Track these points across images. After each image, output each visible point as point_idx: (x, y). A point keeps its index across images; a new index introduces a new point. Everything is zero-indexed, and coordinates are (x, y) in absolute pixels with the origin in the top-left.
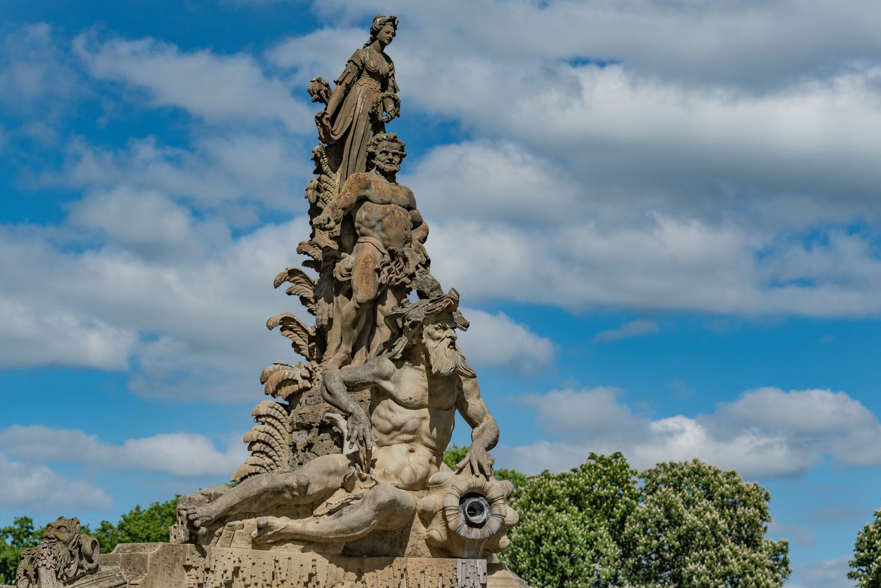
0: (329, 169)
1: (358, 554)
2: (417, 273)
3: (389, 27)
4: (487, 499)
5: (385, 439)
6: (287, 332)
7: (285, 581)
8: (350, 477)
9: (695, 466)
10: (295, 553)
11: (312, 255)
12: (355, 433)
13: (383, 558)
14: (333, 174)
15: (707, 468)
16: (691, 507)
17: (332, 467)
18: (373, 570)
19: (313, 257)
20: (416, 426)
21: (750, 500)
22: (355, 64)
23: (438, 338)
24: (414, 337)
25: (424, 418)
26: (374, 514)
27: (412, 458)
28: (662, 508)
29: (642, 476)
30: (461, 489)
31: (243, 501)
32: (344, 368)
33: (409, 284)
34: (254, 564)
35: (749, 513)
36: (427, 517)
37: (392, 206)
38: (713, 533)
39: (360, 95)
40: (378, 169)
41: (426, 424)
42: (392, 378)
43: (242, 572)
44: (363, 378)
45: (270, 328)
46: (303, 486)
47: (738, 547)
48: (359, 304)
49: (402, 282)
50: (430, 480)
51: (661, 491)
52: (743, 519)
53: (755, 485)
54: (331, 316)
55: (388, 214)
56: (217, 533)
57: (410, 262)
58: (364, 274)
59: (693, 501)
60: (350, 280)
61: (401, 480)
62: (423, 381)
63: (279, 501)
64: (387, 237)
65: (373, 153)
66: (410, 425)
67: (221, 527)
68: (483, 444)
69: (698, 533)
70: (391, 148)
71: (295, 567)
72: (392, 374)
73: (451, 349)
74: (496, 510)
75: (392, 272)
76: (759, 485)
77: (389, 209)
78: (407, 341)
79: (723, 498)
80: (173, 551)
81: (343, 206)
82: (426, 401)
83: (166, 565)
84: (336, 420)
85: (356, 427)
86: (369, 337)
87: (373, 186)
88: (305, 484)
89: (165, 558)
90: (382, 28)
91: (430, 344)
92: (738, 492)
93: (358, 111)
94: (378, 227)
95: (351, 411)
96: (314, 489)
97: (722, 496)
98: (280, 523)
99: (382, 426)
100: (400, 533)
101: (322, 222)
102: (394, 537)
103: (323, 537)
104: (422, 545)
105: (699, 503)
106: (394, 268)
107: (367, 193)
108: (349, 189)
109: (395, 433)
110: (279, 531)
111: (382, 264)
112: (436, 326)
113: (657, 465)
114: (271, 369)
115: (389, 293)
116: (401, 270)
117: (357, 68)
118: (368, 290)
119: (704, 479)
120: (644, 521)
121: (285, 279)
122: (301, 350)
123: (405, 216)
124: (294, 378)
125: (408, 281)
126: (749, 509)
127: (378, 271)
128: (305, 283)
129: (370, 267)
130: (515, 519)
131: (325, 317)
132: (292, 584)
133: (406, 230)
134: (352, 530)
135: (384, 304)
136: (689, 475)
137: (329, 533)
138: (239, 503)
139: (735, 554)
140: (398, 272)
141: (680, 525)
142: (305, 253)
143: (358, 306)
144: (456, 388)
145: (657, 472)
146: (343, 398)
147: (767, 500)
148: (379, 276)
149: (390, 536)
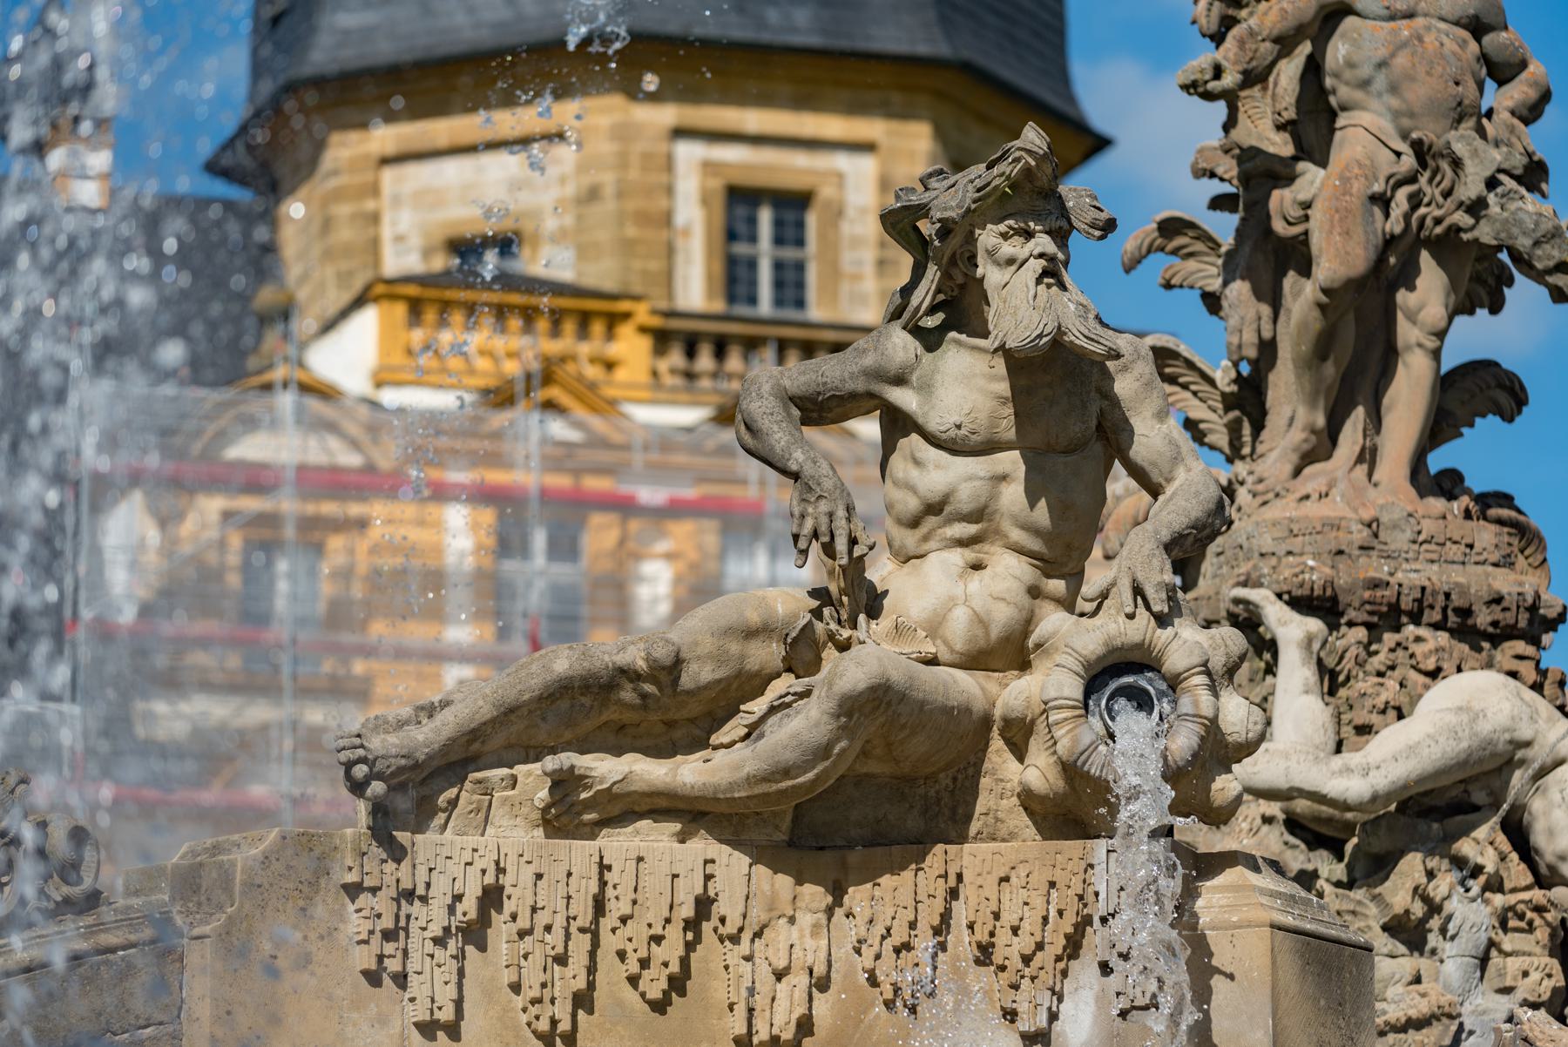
1: (840, 842)
2: (1492, 198)
4: (1164, 678)
5: (909, 539)
7: (631, 917)
8: (795, 640)
10: (661, 844)
12: (809, 525)
13: (896, 849)
17: (754, 617)
18: (870, 875)
20: (983, 500)
23: (1010, 261)
24: (953, 261)
25: (1004, 478)
26: (835, 725)
27: (976, 582)
30: (1084, 652)
31: (505, 714)
32: (1307, 471)
33: (1472, 228)
34: (539, 876)
36: (1018, 734)
37: (1420, 22)
41: (1013, 495)
42: (914, 378)
43: (509, 897)
44: (837, 383)
46: (663, 668)
48: (1325, 291)
49: (1450, 228)
50: (1031, 643)
56: (442, 800)
61: (946, 643)
62: (994, 378)
63: (611, 714)
64: (1404, 107)
66: (966, 497)
67: (452, 786)
68: (1156, 532)
71: (655, 883)
72: (912, 369)
73: (1049, 286)
74: (1185, 705)
75: (1426, 200)
77: (1404, 29)
78: (939, 273)
80: (311, 850)
81: (1275, 32)
82: (1007, 429)
83: (291, 886)
84: (1257, 606)
85: (810, 510)
86: (1378, 384)
88: (668, 661)
89: (289, 867)
91: (992, 276)
94: (1380, 82)
95: (794, 467)
96: (699, 673)
98: (605, 768)
99: (899, 507)
100: (949, 781)
101: (1198, 76)
102: (932, 793)
103: (722, 796)
104: (1010, 811)
106: (1428, 190)
109: (932, 521)
110: (609, 789)
111: (1392, 181)
112: (1002, 227)
115: (1425, 258)
116: (1447, 194)
121: (1151, 245)
122: (1205, 435)
123: (1456, 48)
125: (1470, 221)
127: (1383, 201)
128: (1207, 254)
129: (1354, 190)
130: (1251, 726)
132: (650, 926)
133: (1457, 84)
134: (786, 772)
135: (1411, 288)
137: (732, 786)
138: (493, 722)
142: (1212, 175)
143: (1324, 299)
144: (1093, 394)
146: (777, 436)
148: (1387, 215)
149: (921, 791)
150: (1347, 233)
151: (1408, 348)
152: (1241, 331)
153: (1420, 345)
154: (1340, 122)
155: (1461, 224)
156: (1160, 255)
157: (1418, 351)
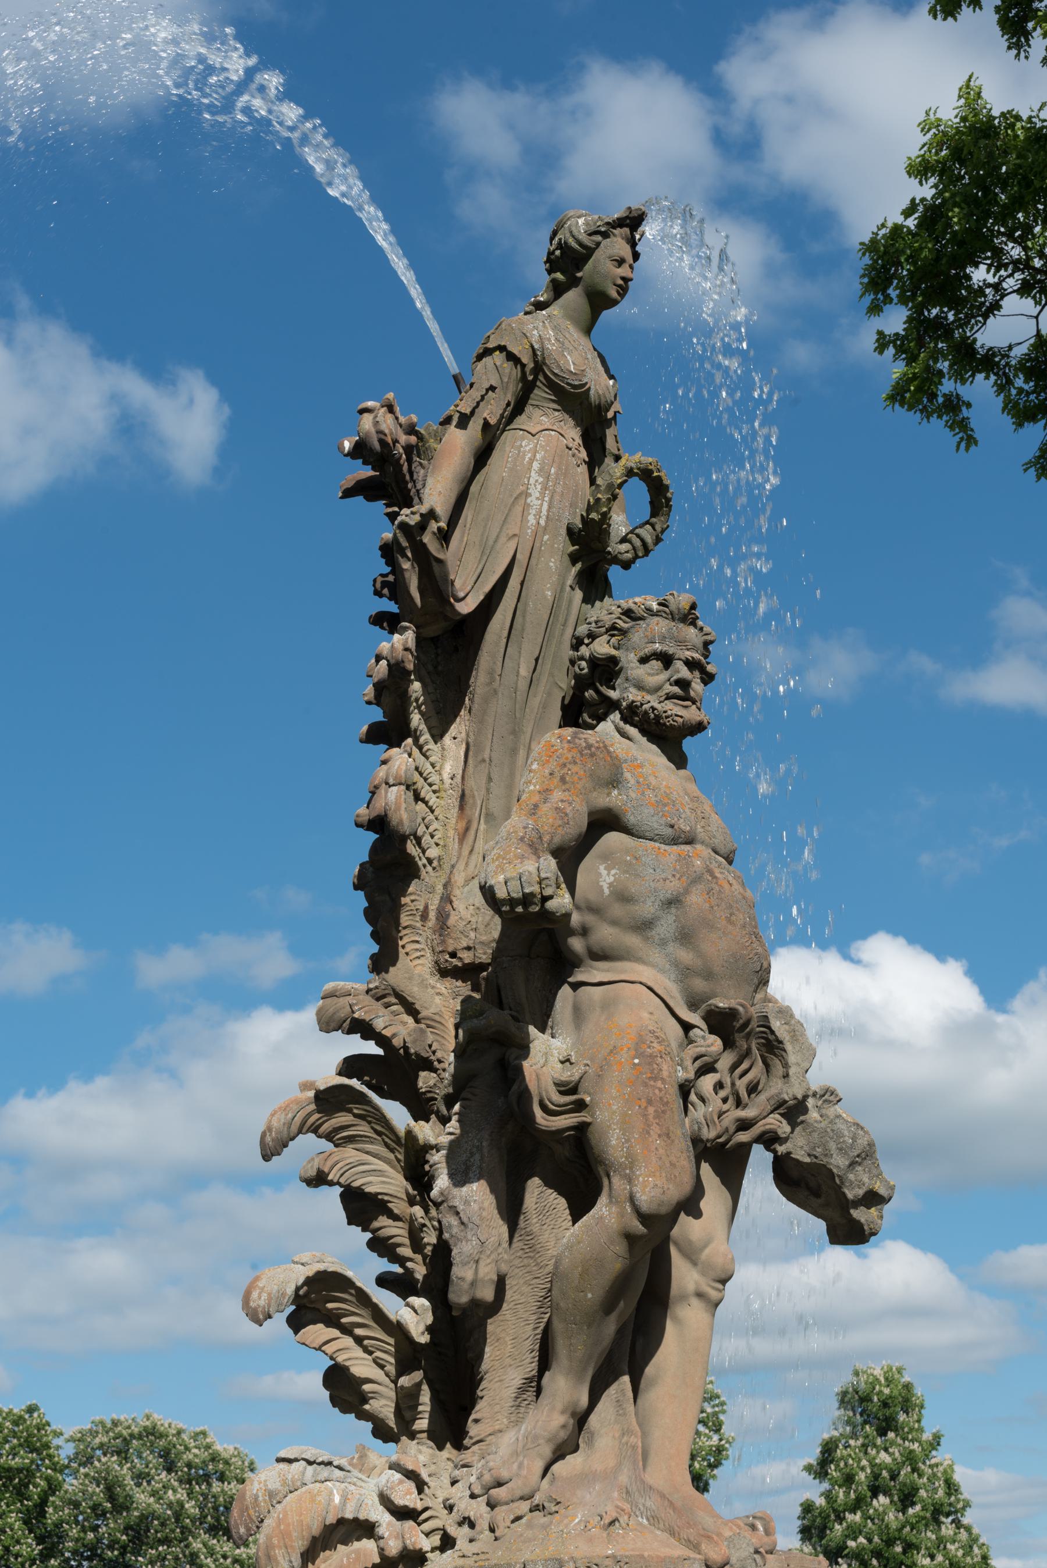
0: (423, 727)
3: (618, 245)
6: (318, 1332)
9: (148, 1423)
11: (387, 1033)
14: (431, 745)
15: (167, 1425)
16: (145, 1484)
19: (382, 1040)
21: (230, 1471)
22: (511, 357)
28: (102, 1486)
29: (71, 1439)
32: (556, 1467)
35: (231, 1489)
38: (177, 1520)
39: (536, 465)
40: (632, 715)
45: (259, 1317)
47: (215, 1541)
48: (644, 1218)
51: (99, 1461)
52: (221, 1499)
53: (235, 1449)
54: (504, 1268)
55: (697, 880)
57: (792, 1058)
58: (650, 1102)
59: (148, 1474)
60: (582, 1128)
64: (699, 962)
65: (613, 660)
69: (156, 1522)
70: (681, 642)
76: (242, 1449)
79: (190, 1469)
81: (557, 840)
87: (627, 775)
90: (598, 244)
92: (213, 1460)
93: (532, 520)
94: (667, 926)
97: (189, 1465)
101: (536, 889)
105: (156, 1478)
106: (727, 1081)
107: (614, 799)
108: (556, 780)
113: (93, 1422)
114: (274, 1484)
117: (517, 372)
118: (672, 1164)
119: (162, 1443)
120: (76, 1505)
124: (362, 1516)
125: (784, 1128)
126: (229, 1483)
129: (665, 1074)
131: (488, 1272)
136: (140, 1437)
139: (211, 1553)
140: (743, 1094)
141: (128, 1509)
142: (363, 1028)
143: (639, 1228)
145: (94, 1434)
147: (252, 1470)
150: (668, 1135)
151: (683, 1297)
152: (477, 1262)
153: (700, 1295)
154: (579, 976)
155: (780, 1132)
156: (311, 1136)
157: (695, 1302)
